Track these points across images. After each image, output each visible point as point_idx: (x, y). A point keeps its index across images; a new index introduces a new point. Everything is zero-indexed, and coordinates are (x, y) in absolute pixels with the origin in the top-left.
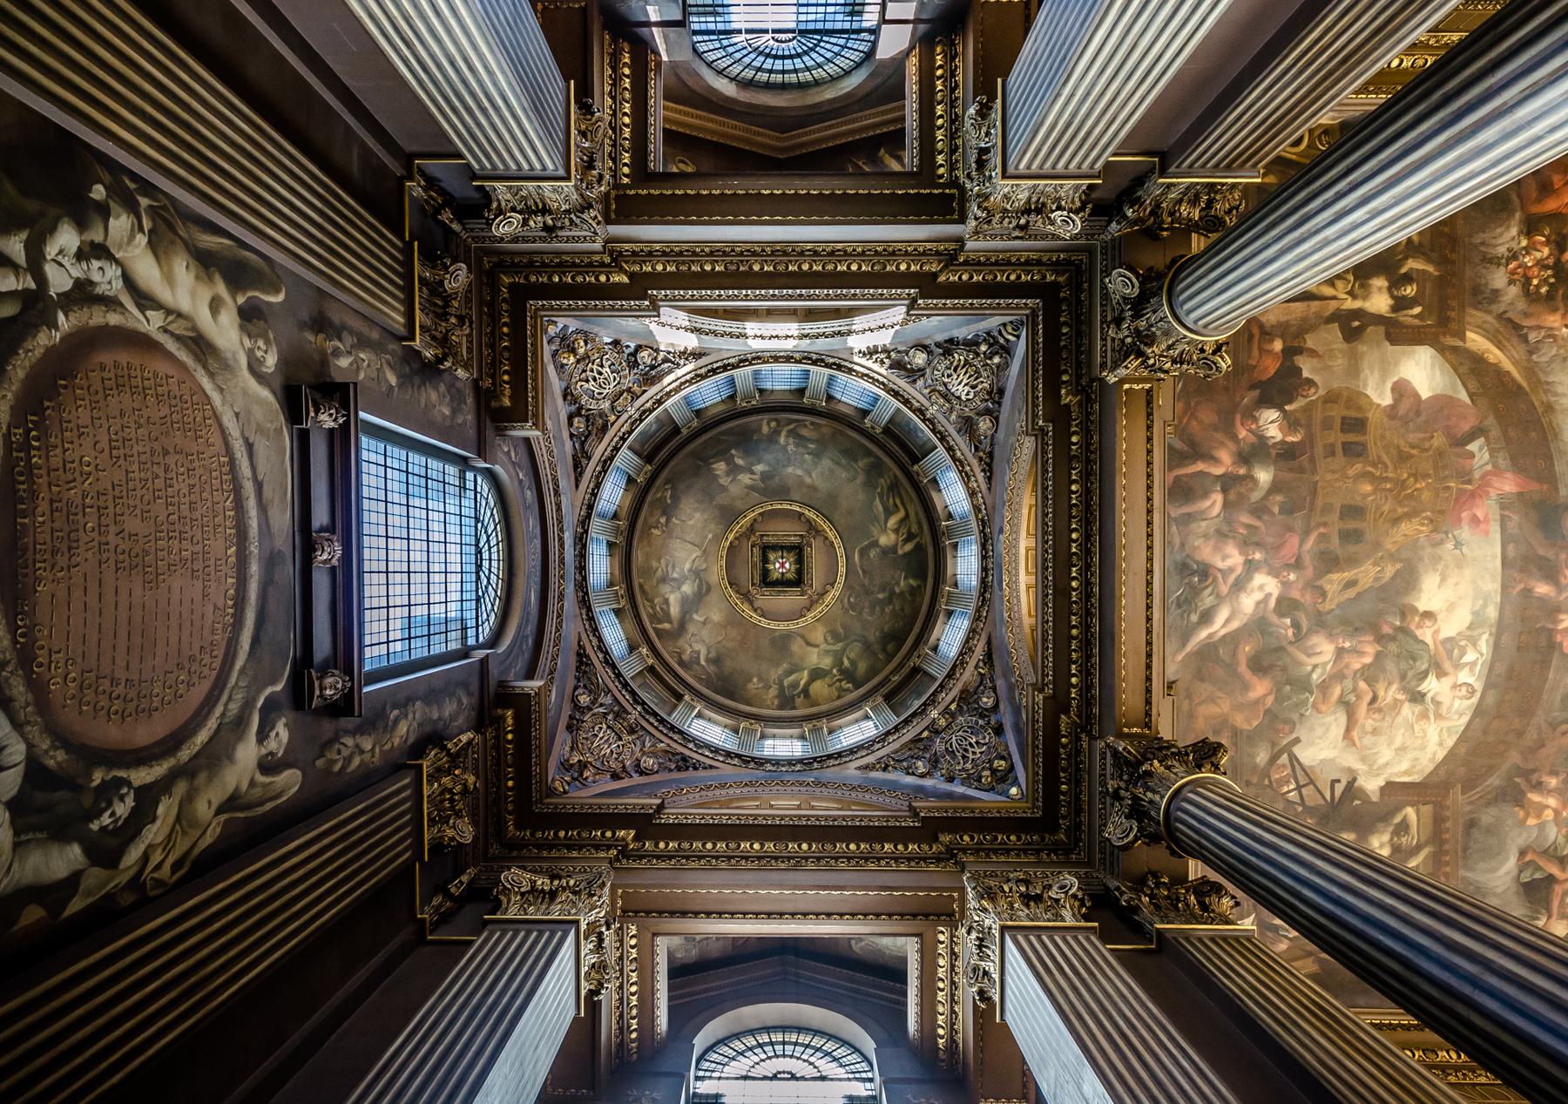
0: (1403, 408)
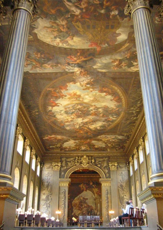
0: (115, 35)
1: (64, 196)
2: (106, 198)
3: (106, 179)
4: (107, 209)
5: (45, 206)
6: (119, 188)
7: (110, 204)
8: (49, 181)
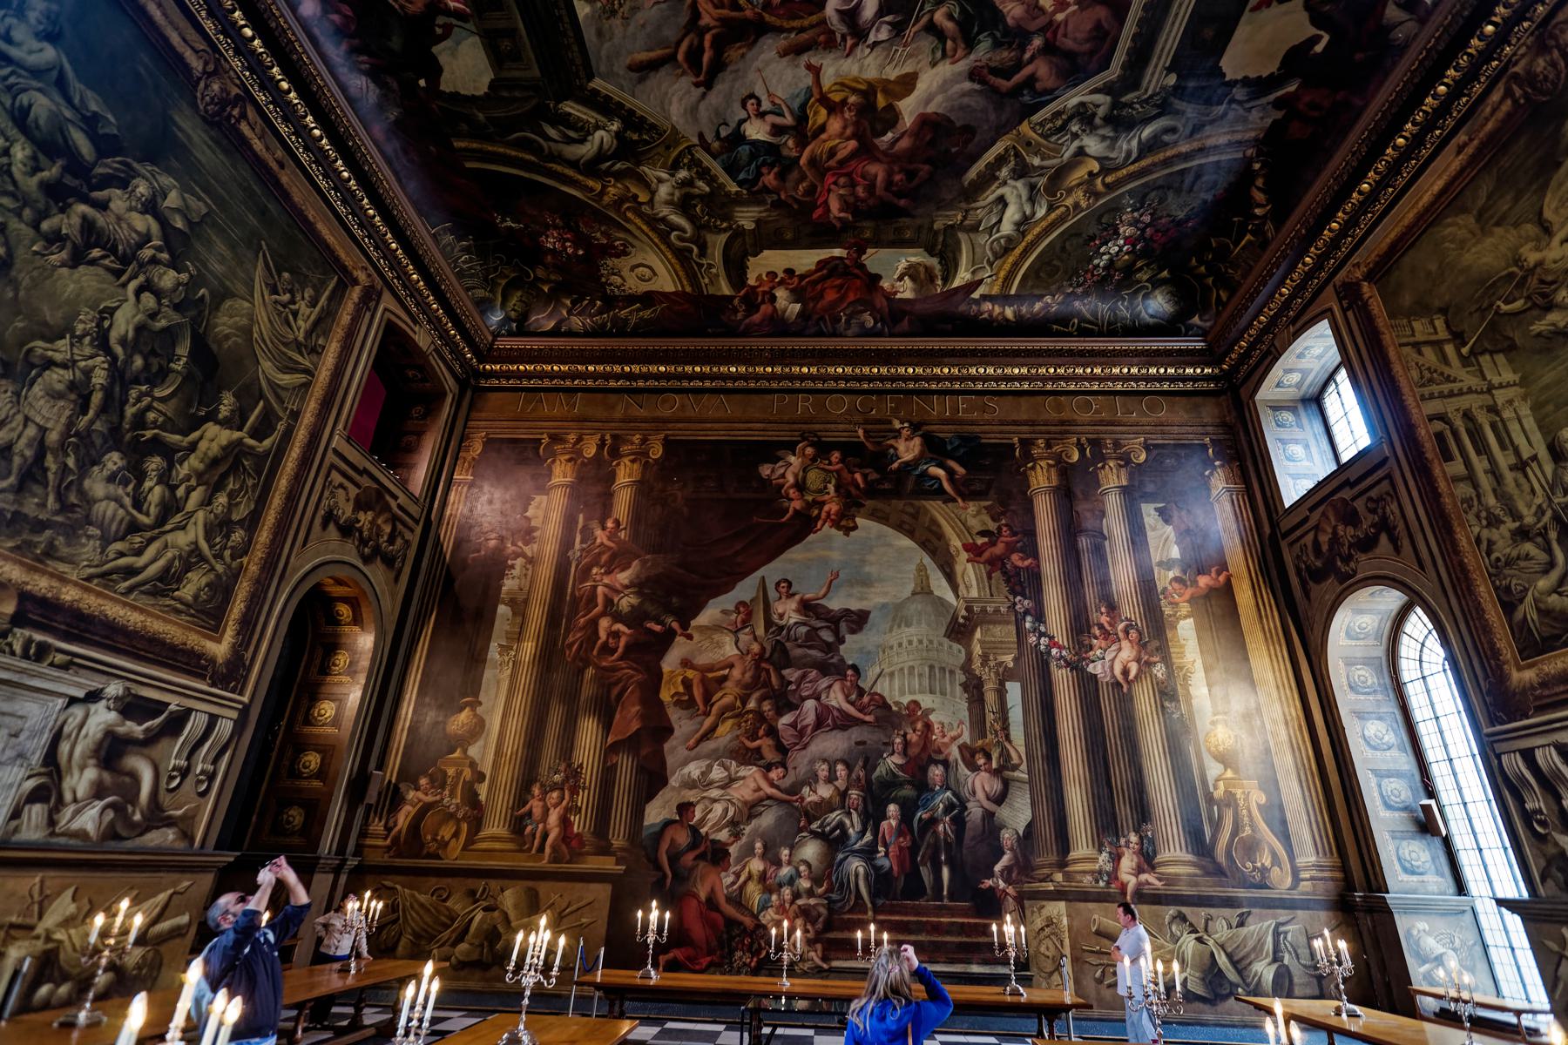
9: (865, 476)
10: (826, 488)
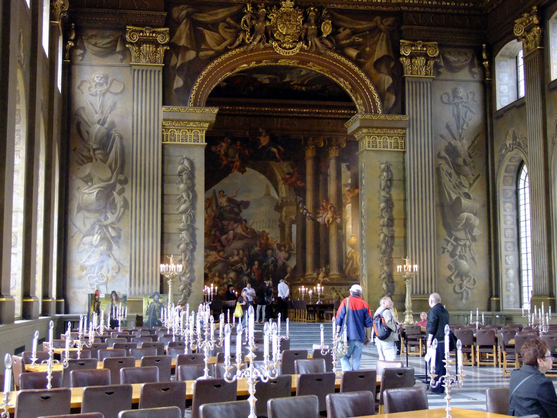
1: (188, 188)
2: (383, 205)
3: (389, 117)
4: (384, 253)
5: (96, 238)
6: (442, 162)
7: (398, 231)
8: (109, 120)
9: (249, 151)
10: (235, 156)
